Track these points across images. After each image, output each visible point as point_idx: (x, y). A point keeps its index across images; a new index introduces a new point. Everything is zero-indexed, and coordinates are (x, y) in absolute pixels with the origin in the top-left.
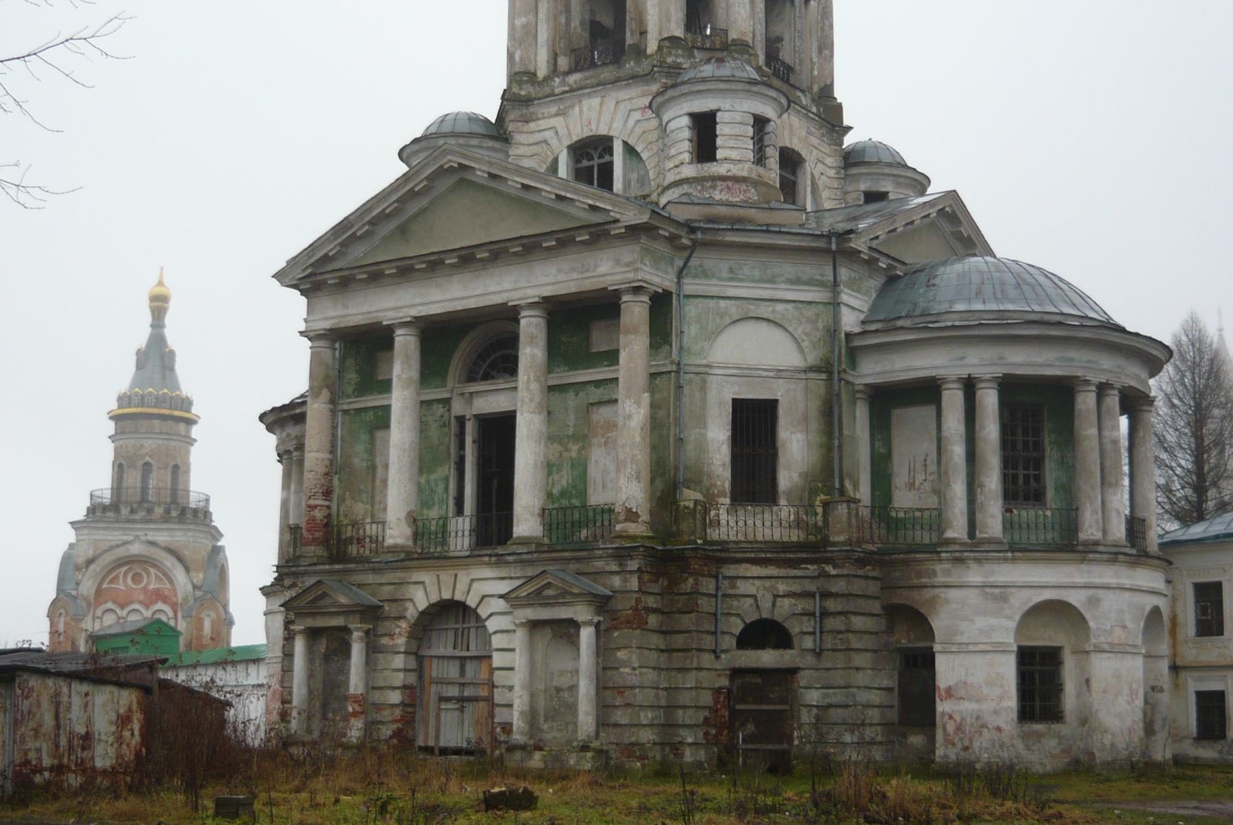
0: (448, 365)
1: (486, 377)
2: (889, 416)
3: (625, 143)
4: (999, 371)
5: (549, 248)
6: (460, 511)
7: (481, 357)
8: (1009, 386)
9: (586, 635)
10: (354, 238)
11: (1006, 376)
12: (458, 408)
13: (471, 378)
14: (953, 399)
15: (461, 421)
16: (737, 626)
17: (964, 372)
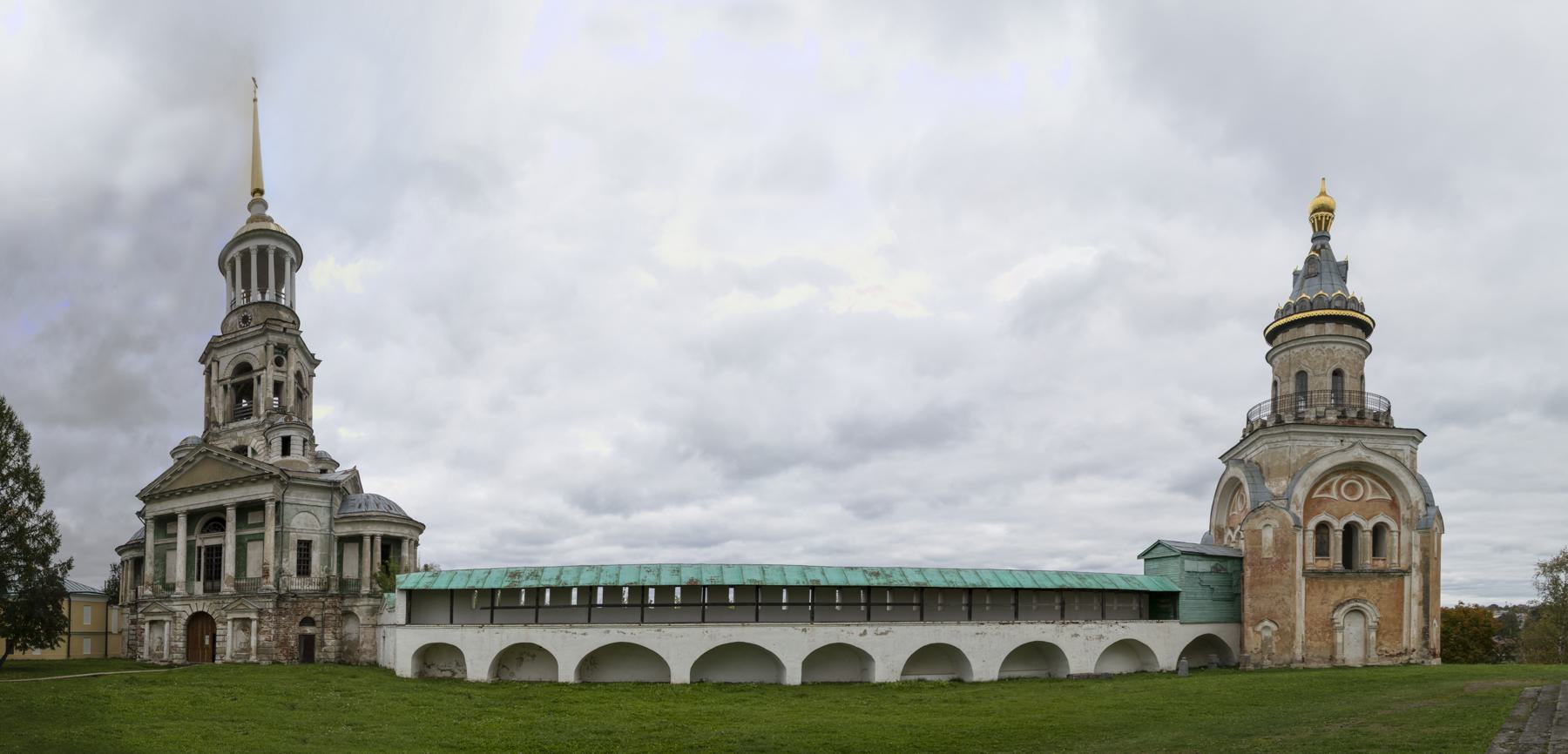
0: (194, 530)
1: (208, 532)
2: (343, 546)
3: (253, 449)
4: (382, 533)
5: (227, 486)
6: (199, 579)
7: (204, 527)
8: (384, 538)
9: (254, 625)
10: (165, 481)
11: (384, 535)
12: (199, 543)
13: (202, 532)
14: (367, 541)
15: (200, 548)
16: (300, 619)
17: (372, 533)
